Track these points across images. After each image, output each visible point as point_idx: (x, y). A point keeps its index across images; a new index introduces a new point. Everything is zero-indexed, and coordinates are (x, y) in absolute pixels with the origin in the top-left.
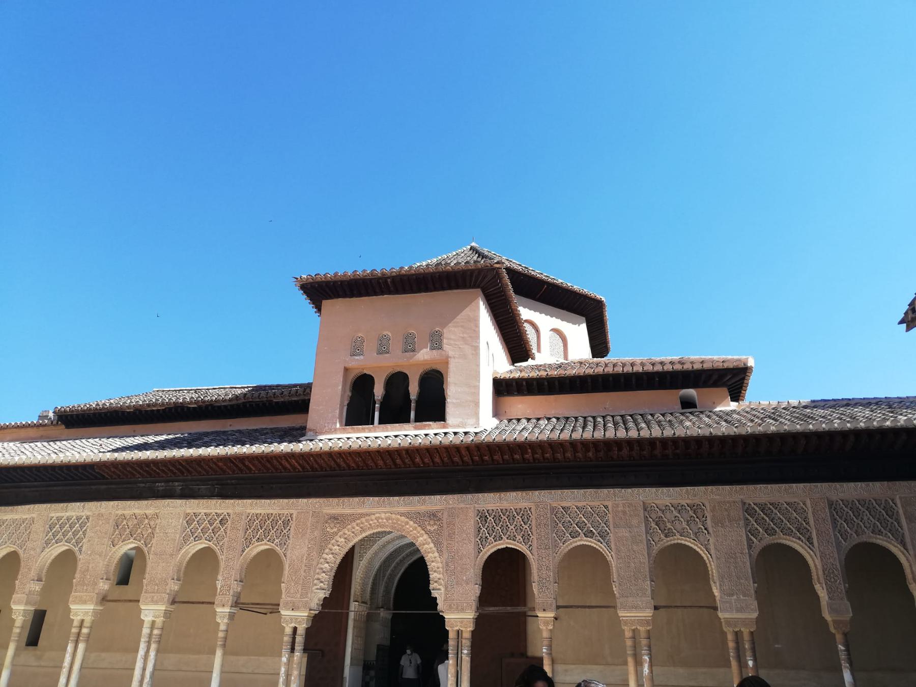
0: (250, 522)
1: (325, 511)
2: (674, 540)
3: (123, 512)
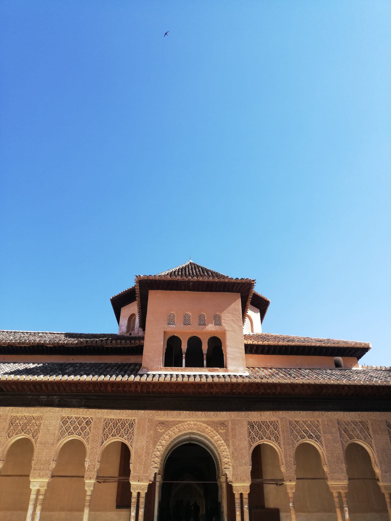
0: (107, 424)
1: (156, 419)
2: (354, 441)
3: (16, 414)
